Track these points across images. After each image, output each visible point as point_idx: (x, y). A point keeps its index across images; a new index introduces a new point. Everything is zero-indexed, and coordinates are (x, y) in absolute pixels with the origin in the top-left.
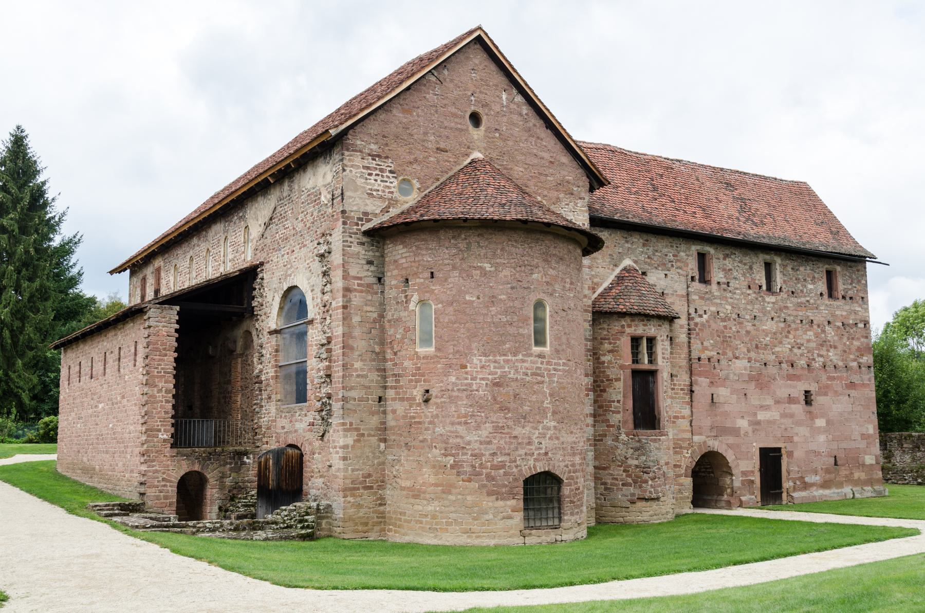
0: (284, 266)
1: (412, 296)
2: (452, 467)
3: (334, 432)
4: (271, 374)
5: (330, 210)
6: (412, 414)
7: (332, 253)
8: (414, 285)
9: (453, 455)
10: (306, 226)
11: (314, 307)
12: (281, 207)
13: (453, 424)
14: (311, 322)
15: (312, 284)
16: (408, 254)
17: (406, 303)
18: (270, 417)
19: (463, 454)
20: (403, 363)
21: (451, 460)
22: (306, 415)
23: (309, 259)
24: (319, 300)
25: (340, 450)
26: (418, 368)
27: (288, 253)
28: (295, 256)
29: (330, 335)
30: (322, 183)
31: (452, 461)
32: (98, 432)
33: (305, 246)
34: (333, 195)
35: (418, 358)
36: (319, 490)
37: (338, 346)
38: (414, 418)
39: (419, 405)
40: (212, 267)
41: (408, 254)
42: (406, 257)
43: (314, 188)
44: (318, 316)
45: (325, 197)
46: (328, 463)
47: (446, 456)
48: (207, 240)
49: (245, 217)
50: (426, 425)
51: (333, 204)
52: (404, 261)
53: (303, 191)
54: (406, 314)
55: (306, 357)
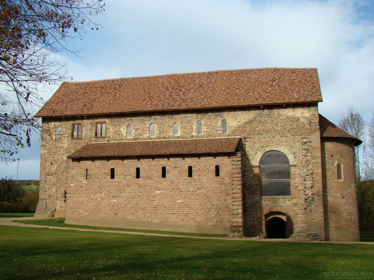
0: (266, 142)
1: (335, 161)
2: (350, 219)
3: (316, 206)
4: (254, 184)
5: (308, 127)
6: (337, 202)
7: (312, 143)
8: (336, 158)
9: (349, 216)
10: (286, 129)
11: (295, 160)
12: (260, 118)
13: (349, 205)
14: (295, 166)
15: (293, 151)
16: (333, 147)
17: (333, 163)
18: (254, 200)
19: (352, 216)
20: (332, 184)
21: (349, 217)
22: (289, 200)
23: (290, 142)
24: (301, 158)
25: (321, 213)
26: (338, 186)
27: (269, 137)
28: (276, 139)
29: (312, 172)
30: (301, 116)
31: (350, 218)
32: (155, 203)
33: (284, 136)
34: (310, 122)
35: (338, 183)
36: (303, 228)
37: (319, 176)
38: (337, 203)
39: (339, 199)
40: (182, 132)
41: (333, 147)
42: (332, 148)
43: (292, 116)
44: (300, 165)
45: (304, 121)
46: (312, 218)
47: (348, 216)
48: (172, 119)
49: (222, 115)
50: (342, 206)
51: (310, 125)
52: (331, 149)
53: (282, 115)
54: (333, 167)
55: (290, 178)
